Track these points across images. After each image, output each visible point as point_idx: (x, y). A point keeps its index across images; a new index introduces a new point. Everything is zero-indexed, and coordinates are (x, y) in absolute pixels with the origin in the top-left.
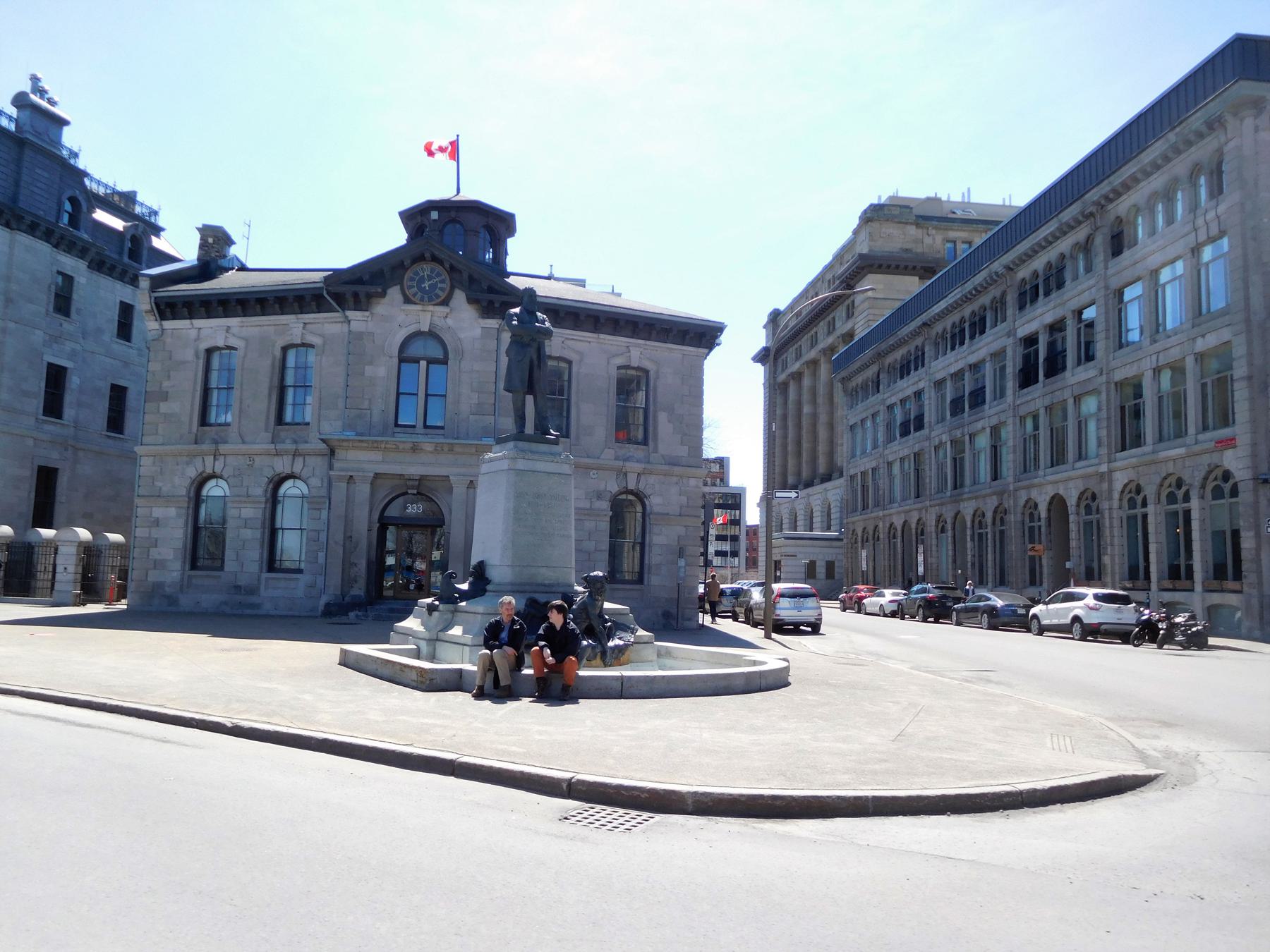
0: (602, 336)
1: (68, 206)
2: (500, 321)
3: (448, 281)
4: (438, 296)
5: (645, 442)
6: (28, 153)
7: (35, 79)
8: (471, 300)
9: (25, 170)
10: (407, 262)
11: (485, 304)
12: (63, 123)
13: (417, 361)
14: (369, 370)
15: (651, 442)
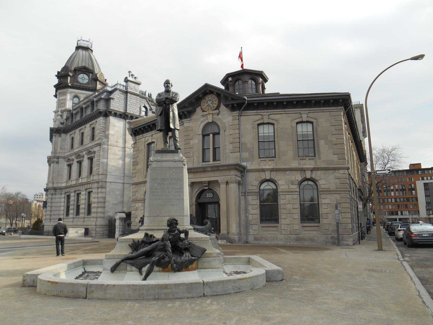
1: (144, 109)
2: (238, 112)
4: (214, 107)
6: (129, 95)
8: (227, 106)
9: (128, 101)
11: (230, 106)
13: (208, 135)
14: (192, 142)
15: (317, 155)
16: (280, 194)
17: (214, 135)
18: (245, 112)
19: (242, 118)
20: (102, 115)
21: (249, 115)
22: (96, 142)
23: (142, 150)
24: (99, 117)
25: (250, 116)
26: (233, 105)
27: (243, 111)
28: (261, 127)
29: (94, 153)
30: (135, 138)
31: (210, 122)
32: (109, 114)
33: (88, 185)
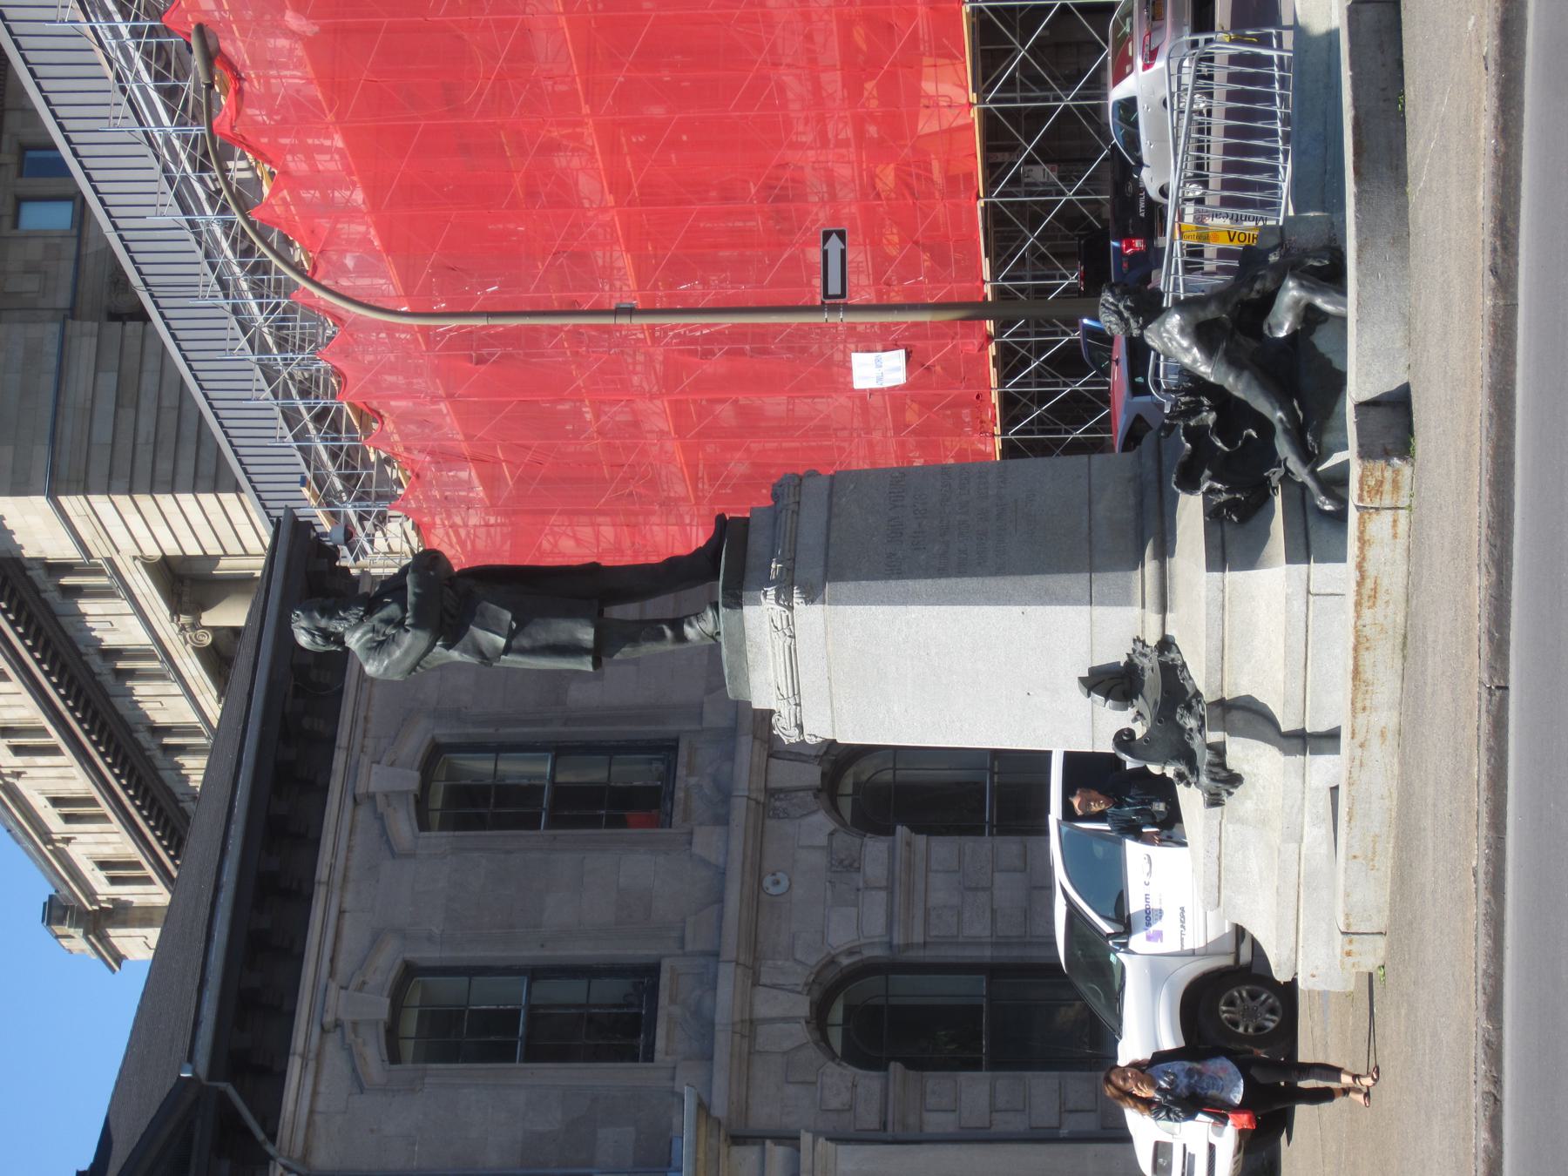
0: (322, 873)
5: (666, 749)
15: (671, 728)
18: (284, 1132)
21: (312, 1112)
25: (321, 1105)
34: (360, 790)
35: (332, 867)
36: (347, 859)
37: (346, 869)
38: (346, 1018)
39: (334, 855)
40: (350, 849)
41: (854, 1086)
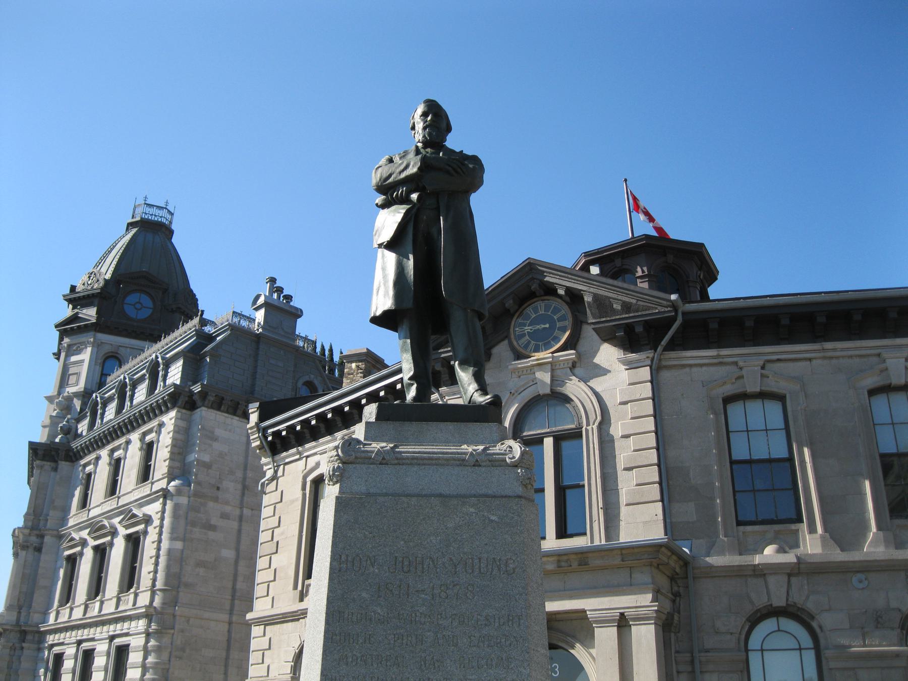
0: (829, 345)
2: (650, 354)
3: (570, 316)
7: (273, 280)
10: (509, 303)
12: (297, 314)
16: (832, 665)
17: (559, 439)
18: (673, 354)
19: (665, 375)
20: (180, 403)
21: (691, 366)
22: (156, 487)
23: (292, 502)
24: (168, 410)
25: (695, 369)
26: (629, 329)
27: (666, 349)
28: (736, 410)
29: (148, 520)
30: (274, 461)
31: (545, 395)
32: (199, 403)
33: (119, 626)
34: (885, 354)
35: (834, 350)
36: (843, 357)
37: (837, 358)
38: (744, 372)
39: (842, 350)
40: (851, 357)
41: (731, 634)
